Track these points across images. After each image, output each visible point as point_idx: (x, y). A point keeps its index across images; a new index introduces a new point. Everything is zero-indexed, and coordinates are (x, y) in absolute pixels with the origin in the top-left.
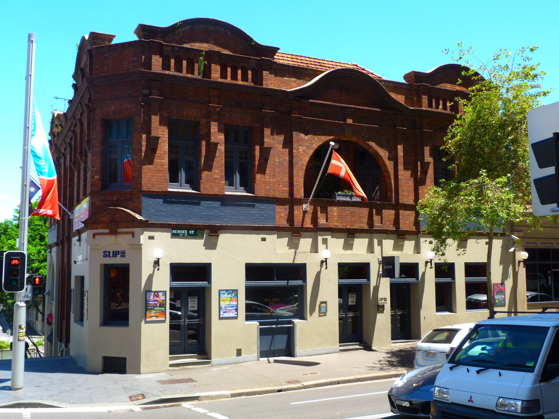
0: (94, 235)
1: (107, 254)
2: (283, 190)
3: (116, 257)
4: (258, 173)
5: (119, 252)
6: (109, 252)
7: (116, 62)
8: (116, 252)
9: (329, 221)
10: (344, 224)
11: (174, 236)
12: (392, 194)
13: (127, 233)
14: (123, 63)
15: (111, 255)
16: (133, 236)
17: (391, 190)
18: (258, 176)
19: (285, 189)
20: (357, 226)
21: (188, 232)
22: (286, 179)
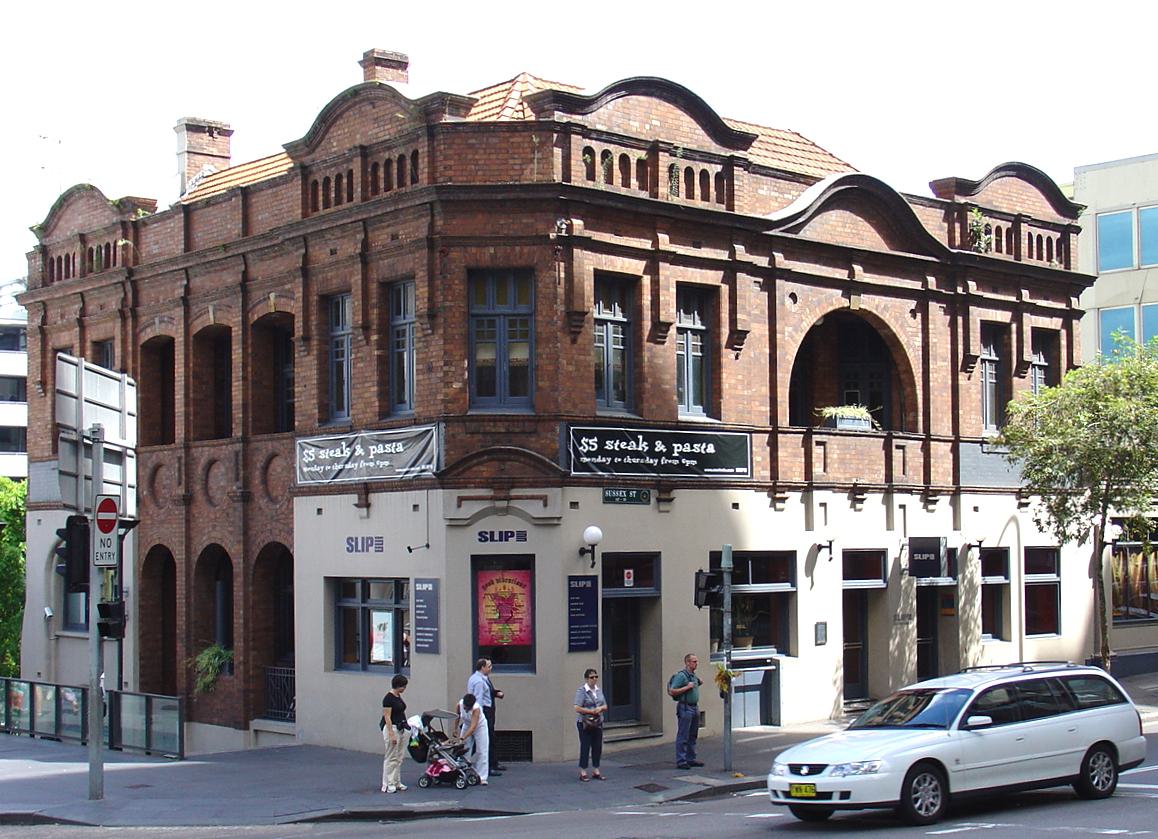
0: (461, 499)
1: (488, 536)
2: (760, 411)
3: (507, 540)
4: (1015, 376)
5: (512, 533)
6: (357, 539)
7: (493, 157)
8: (507, 532)
9: (828, 469)
10: (848, 476)
11: (834, 492)
12: (916, 416)
13: (532, 498)
14: (511, 162)
15: (496, 537)
16: (545, 505)
17: (916, 410)
18: (1015, 379)
19: (763, 409)
20: (864, 481)
21: (628, 494)
22: (766, 390)
